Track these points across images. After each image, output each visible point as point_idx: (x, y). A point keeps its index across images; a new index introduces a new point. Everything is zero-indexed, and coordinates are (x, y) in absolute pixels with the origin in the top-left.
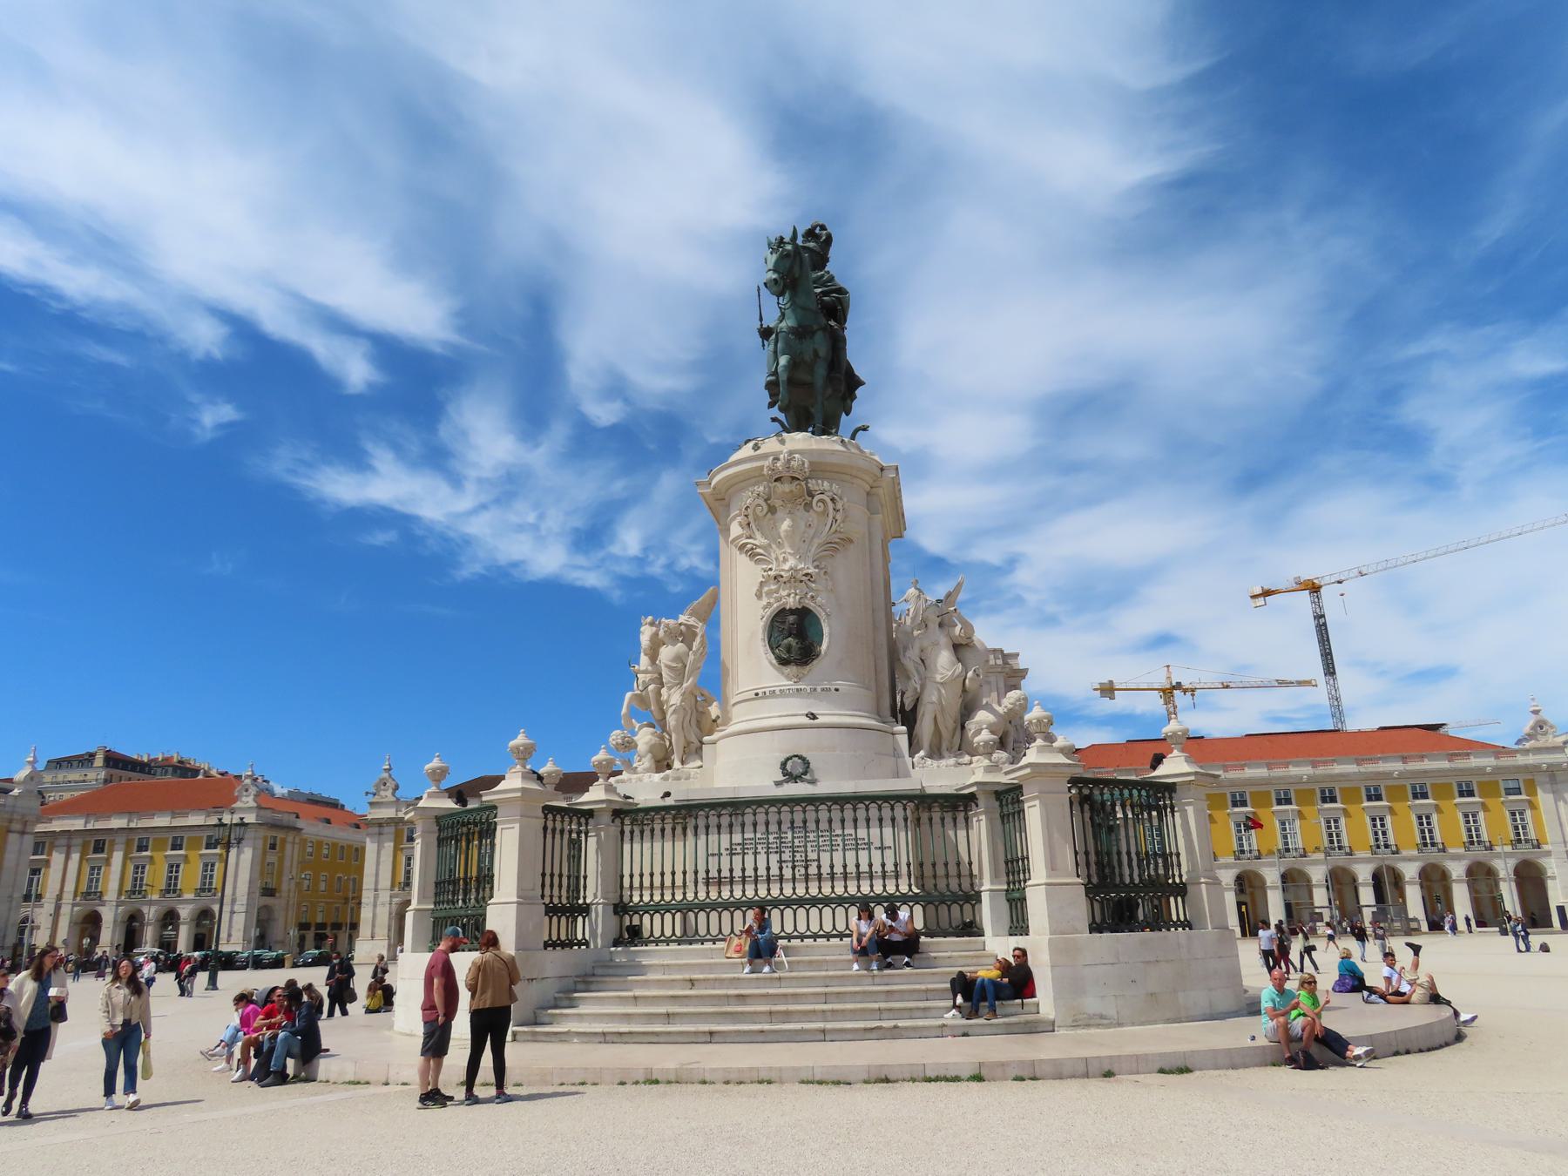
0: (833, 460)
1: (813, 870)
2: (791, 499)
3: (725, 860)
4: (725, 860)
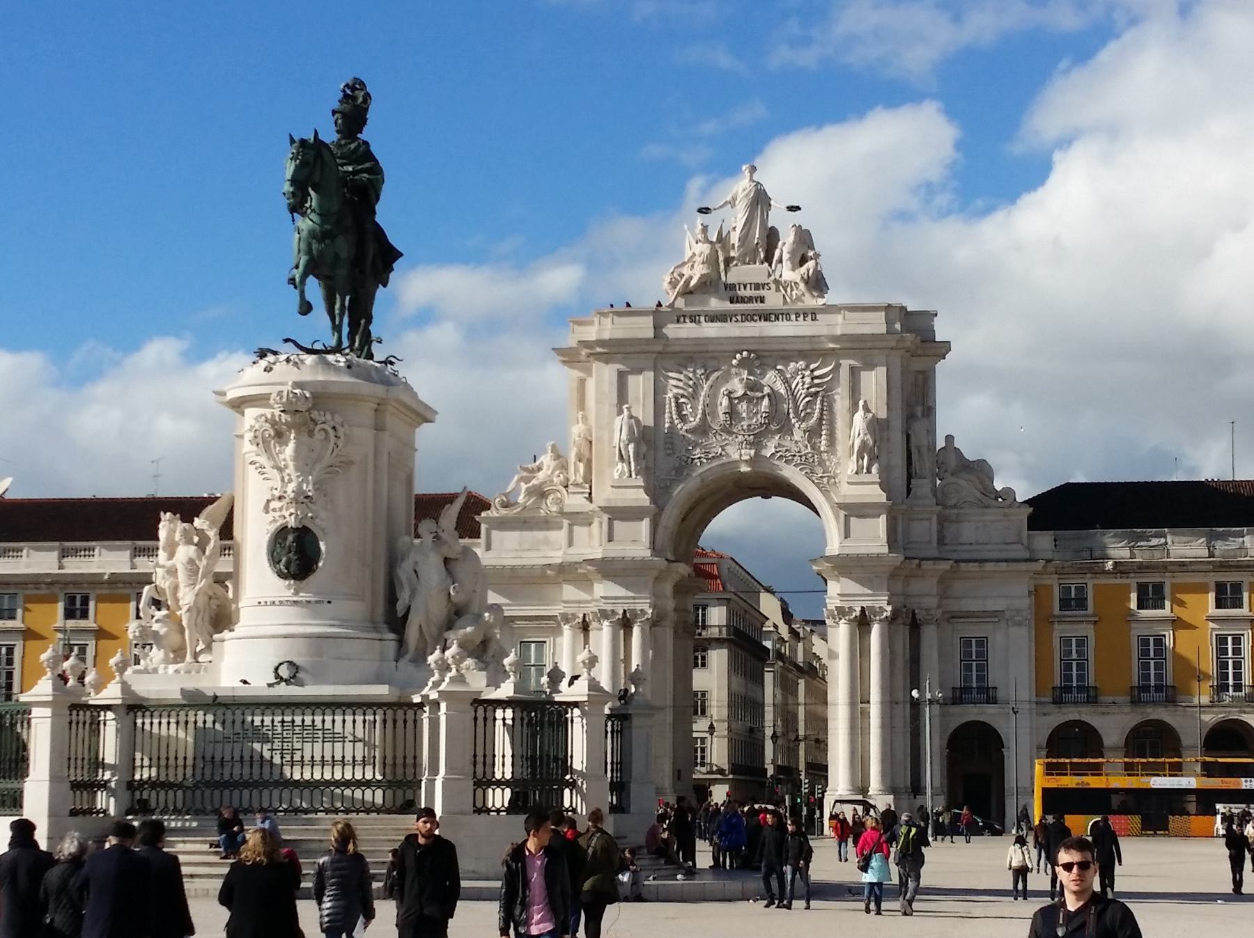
0: (335, 389)
1: (297, 757)
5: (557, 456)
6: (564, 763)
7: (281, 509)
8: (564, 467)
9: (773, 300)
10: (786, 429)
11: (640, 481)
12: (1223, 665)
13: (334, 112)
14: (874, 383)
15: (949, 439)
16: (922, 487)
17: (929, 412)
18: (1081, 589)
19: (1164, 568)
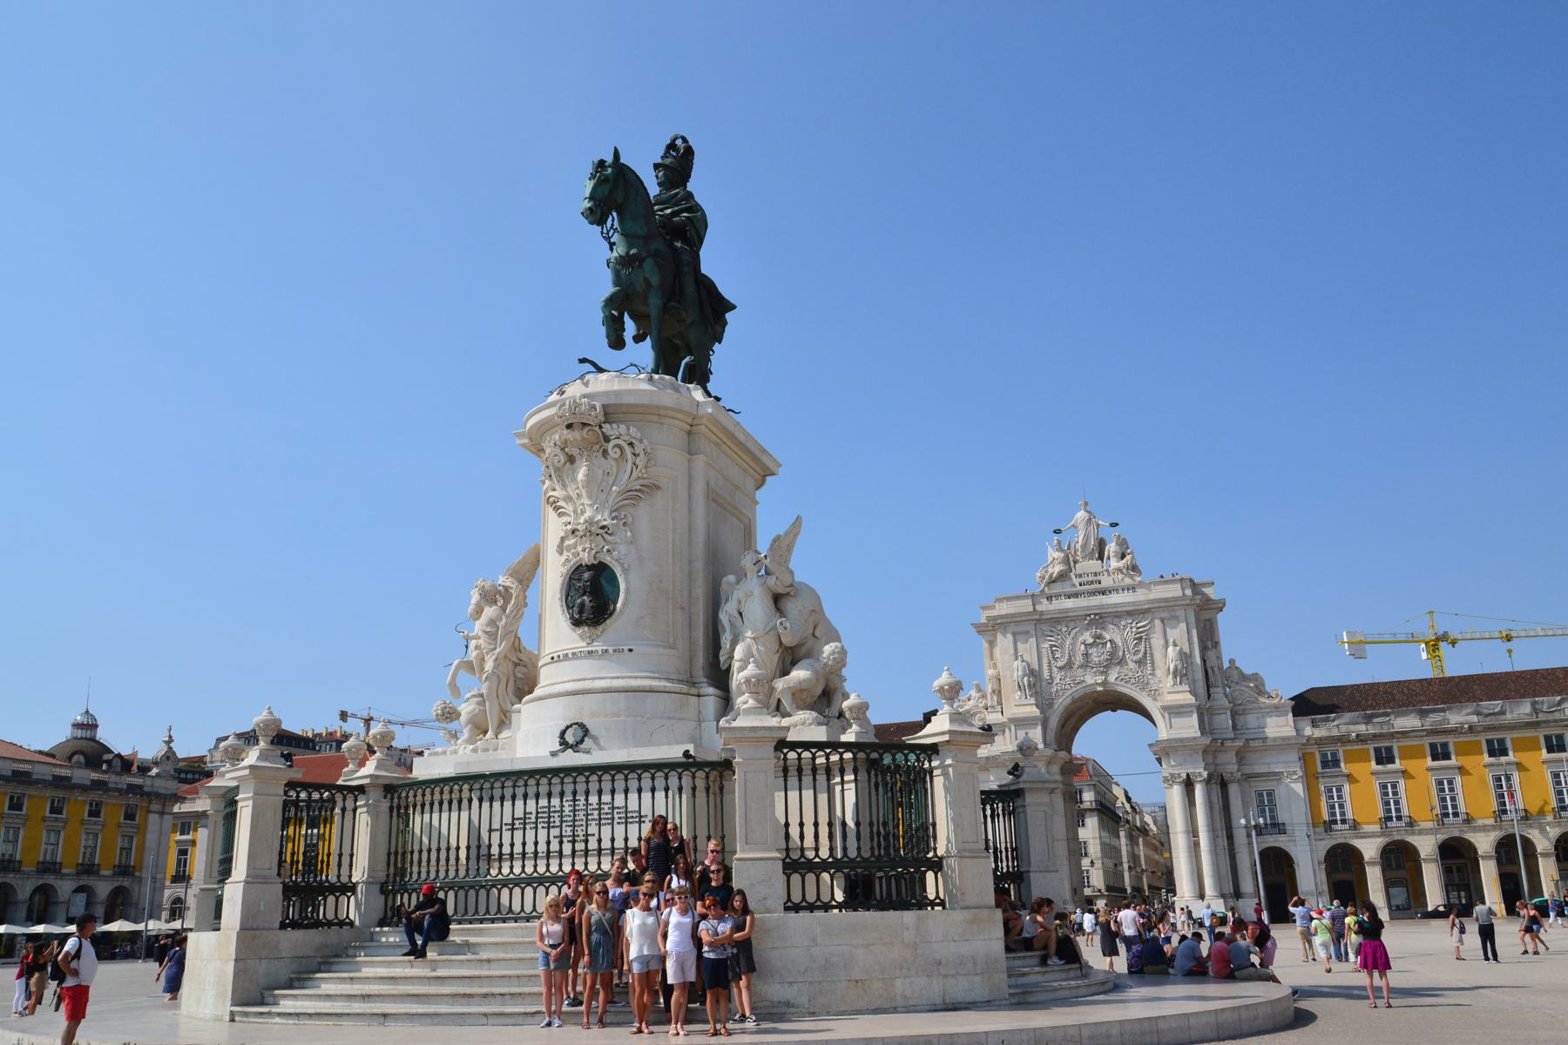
0: (632, 400)
2: (587, 448)
3: (507, 835)
4: (507, 835)
5: (979, 690)
6: (924, 833)
7: (575, 546)
8: (984, 697)
9: (1107, 582)
10: (1122, 662)
11: (1033, 701)
12: (1444, 800)
13: (656, 166)
14: (1178, 633)
15: (1232, 662)
16: (1218, 692)
17: (1216, 644)
18: (1334, 754)
19: (1392, 736)
